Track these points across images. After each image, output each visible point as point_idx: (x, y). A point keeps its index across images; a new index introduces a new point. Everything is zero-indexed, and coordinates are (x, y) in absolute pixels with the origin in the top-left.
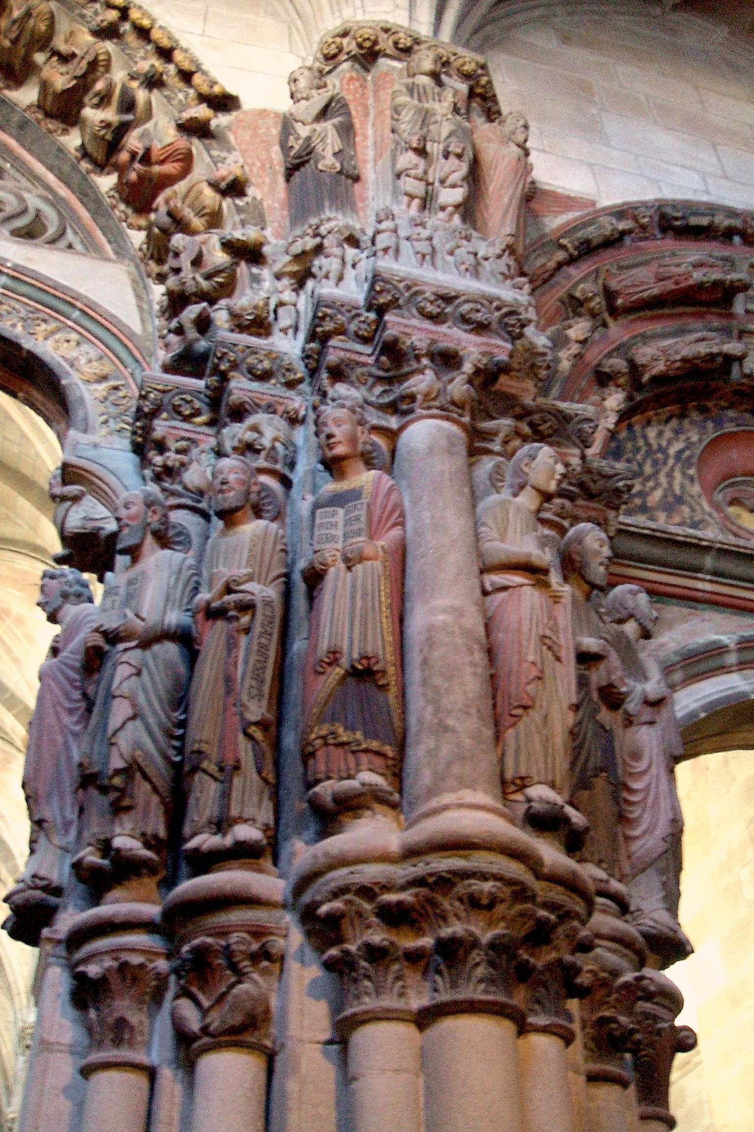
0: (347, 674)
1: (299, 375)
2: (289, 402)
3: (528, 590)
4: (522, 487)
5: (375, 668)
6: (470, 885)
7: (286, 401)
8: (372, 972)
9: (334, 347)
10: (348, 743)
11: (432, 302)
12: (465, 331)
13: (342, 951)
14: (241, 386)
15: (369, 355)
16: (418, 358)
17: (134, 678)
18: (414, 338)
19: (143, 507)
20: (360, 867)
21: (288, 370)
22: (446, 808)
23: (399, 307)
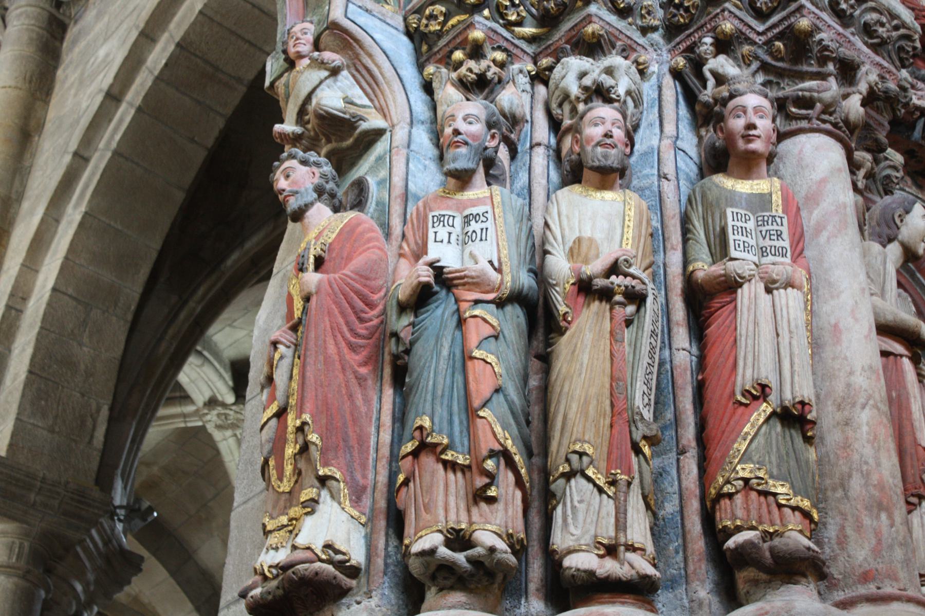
0: (774, 413)
1: (656, 23)
2: (643, 51)
4: (890, 240)
5: (809, 417)
7: (638, 48)
9: (730, 12)
10: (775, 495)
12: (866, 43)
15: (759, 34)
16: (823, 61)
17: (492, 340)
18: (822, 35)
19: (485, 129)
21: (649, 13)
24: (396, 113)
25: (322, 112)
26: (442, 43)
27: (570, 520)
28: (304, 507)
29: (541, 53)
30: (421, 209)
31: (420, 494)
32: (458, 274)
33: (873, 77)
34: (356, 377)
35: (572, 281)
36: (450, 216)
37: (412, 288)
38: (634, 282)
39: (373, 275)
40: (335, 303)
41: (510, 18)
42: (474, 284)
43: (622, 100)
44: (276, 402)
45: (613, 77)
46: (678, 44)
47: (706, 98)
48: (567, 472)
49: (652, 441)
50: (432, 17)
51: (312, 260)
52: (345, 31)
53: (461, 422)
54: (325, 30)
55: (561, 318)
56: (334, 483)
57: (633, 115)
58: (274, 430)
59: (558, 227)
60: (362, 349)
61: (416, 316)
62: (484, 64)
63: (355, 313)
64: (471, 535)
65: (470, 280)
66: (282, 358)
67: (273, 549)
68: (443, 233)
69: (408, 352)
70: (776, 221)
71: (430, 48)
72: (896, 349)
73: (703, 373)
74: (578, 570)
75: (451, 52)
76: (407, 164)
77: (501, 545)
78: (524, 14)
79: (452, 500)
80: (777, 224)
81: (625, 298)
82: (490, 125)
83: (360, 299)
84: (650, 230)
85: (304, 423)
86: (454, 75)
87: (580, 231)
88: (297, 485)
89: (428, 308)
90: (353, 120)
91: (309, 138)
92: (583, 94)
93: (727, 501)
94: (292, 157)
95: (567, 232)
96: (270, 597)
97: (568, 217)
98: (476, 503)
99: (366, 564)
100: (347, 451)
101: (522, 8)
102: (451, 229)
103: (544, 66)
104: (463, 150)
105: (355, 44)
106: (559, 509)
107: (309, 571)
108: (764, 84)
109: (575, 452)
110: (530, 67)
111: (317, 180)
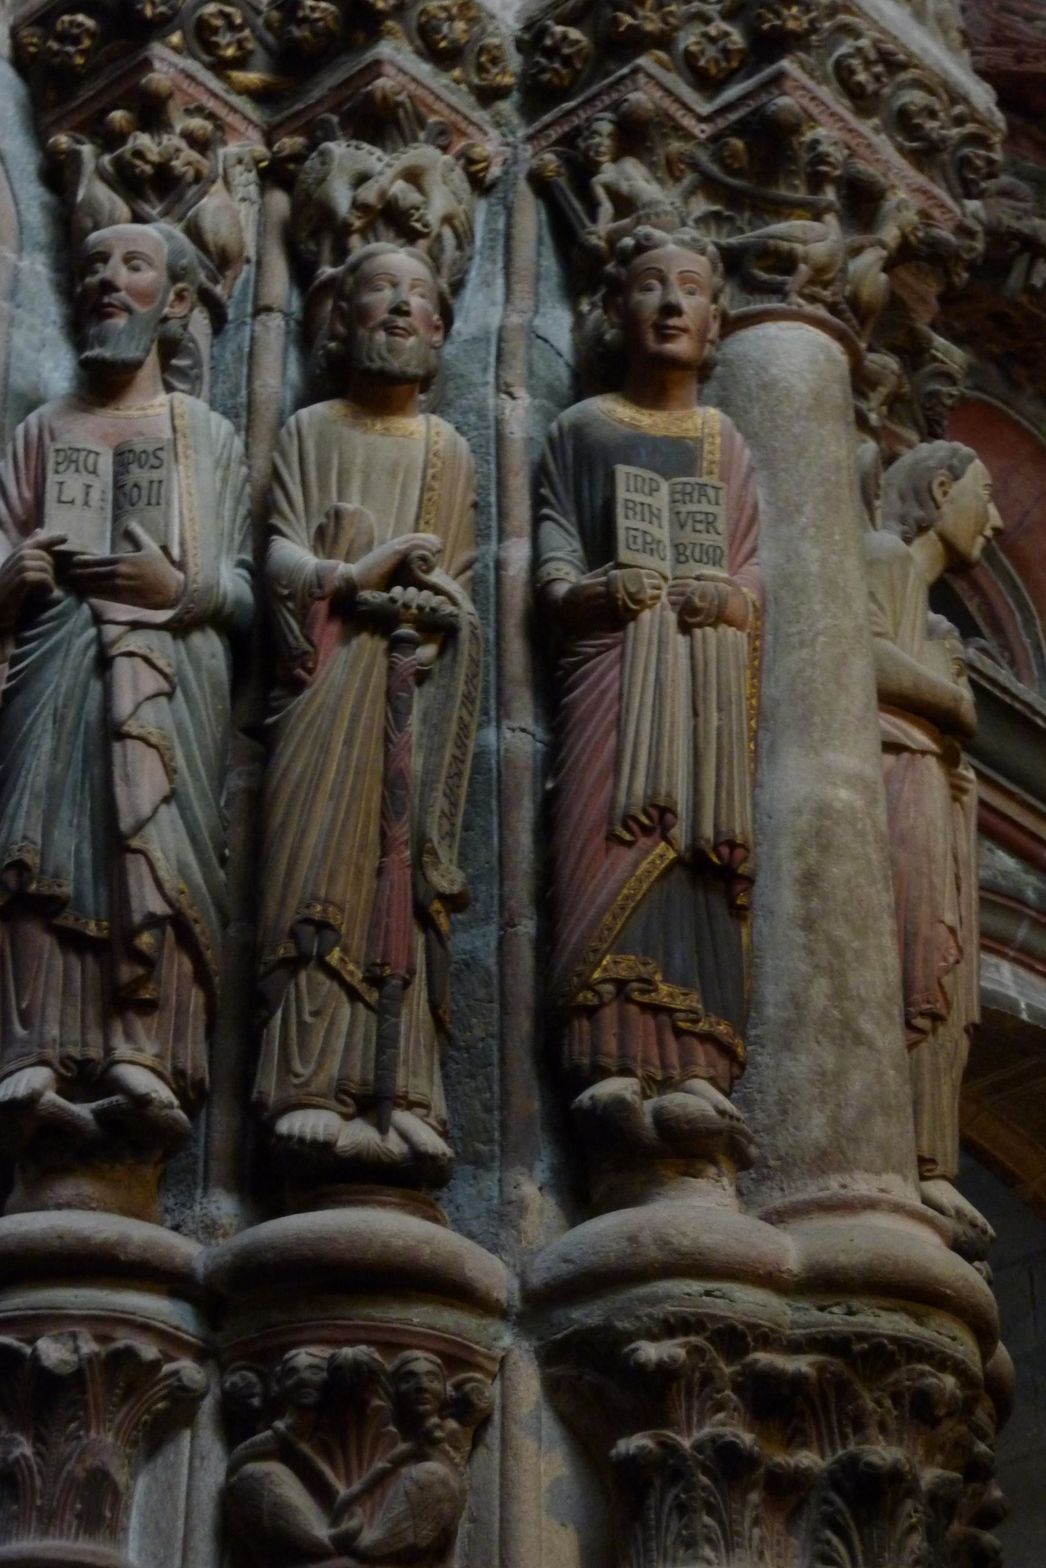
0: (678, 861)
1: (508, 80)
2: (478, 137)
3: (932, 762)
4: (922, 529)
5: (741, 870)
6: (922, 1374)
7: (471, 130)
8: (717, 1499)
9: (649, 76)
10: (670, 1011)
11: (868, 64)
12: (900, 149)
13: (662, 1444)
14: (400, 59)
15: (702, 119)
16: (816, 182)
17: (163, 700)
18: (821, 132)
19: (164, 279)
20: (726, 1286)
22: (871, 1205)
23: (807, 48)
26: (85, 93)
27: (295, 1049)
29: (280, 125)
33: (911, 216)
36: (90, 452)
38: (436, 600)
41: (221, 53)
43: (434, 234)
45: (421, 190)
46: (548, 126)
47: (594, 240)
49: (455, 903)
57: (454, 263)
62: (173, 140)
68: (74, 484)
70: (706, 495)
72: (913, 739)
73: (555, 776)
77: (163, 1092)
78: (250, 45)
80: (709, 502)
81: (418, 630)
82: (175, 275)
84: (472, 497)
93: (586, 1023)
101: (247, 32)
102: (88, 479)
108: (703, 221)
109: (308, 921)
110: (260, 149)
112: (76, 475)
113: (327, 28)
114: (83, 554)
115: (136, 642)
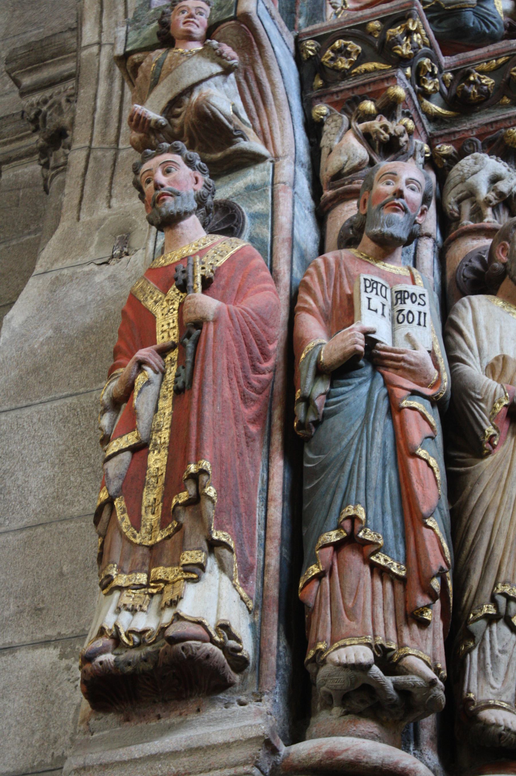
24: (283, 144)
25: (208, 111)
26: (345, 85)
28: (186, 571)
29: (441, 136)
30: (333, 265)
31: (340, 595)
32: (394, 355)
34: (246, 434)
35: (506, 402)
37: (344, 354)
39: (271, 322)
40: (234, 339)
41: (426, 86)
42: (410, 371)
44: (136, 433)
48: (492, 615)
50: (343, 52)
51: (199, 280)
52: (253, 30)
53: (395, 525)
54: (231, 19)
55: (487, 439)
56: (227, 553)
58: (126, 466)
59: (474, 336)
60: (252, 403)
61: (332, 387)
63: (251, 359)
64: (401, 659)
65: (407, 366)
66: (149, 382)
67: (128, 610)
68: (376, 302)
69: (317, 424)
71: (326, 85)
74: (509, 730)
75: (363, 98)
76: (293, 206)
79: (379, 611)
83: (258, 345)
85: (203, 472)
86: (361, 127)
87: (502, 349)
88: (169, 542)
89: (350, 381)
90: (235, 134)
91: (169, 134)
92: (495, 199)
94: (176, 151)
95: (485, 345)
96: (129, 669)
97: (486, 329)
98: (408, 624)
99: (254, 659)
100: (237, 519)
103: (445, 152)
104: (400, 216)
105: (256, 49)
106: (475, 653)
107: (200, 650)
111: (200, 188)
112: (377, 296)
113: (488, 90)
114: (382, 343)
115: (416, 403)
